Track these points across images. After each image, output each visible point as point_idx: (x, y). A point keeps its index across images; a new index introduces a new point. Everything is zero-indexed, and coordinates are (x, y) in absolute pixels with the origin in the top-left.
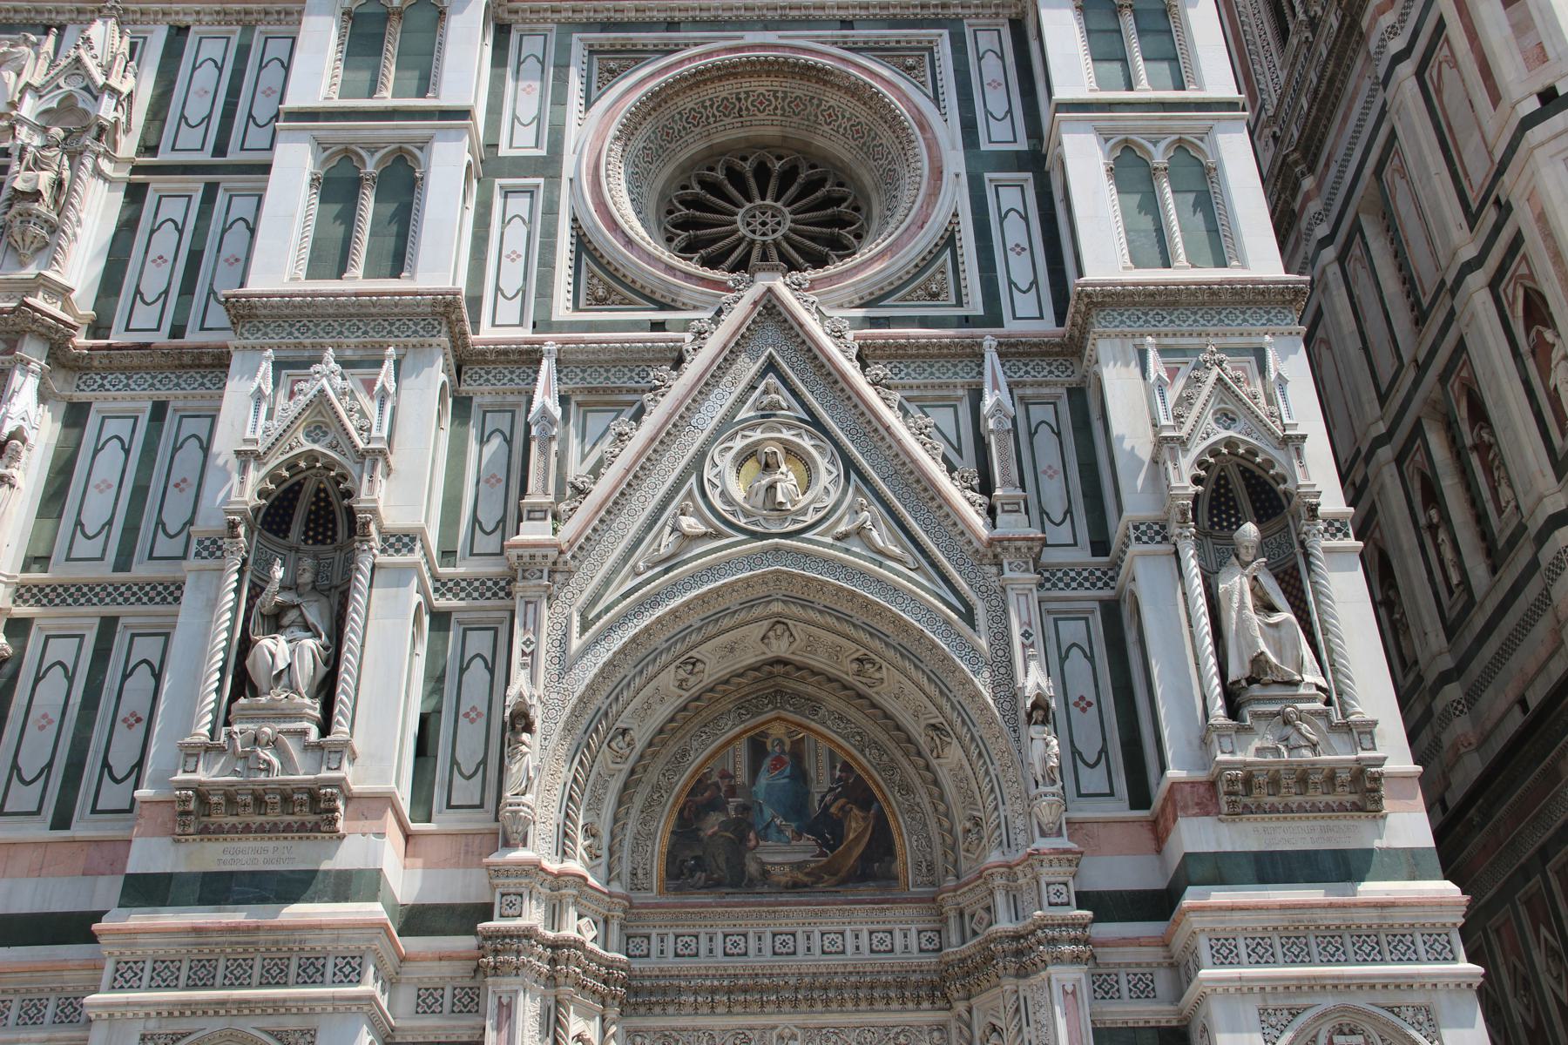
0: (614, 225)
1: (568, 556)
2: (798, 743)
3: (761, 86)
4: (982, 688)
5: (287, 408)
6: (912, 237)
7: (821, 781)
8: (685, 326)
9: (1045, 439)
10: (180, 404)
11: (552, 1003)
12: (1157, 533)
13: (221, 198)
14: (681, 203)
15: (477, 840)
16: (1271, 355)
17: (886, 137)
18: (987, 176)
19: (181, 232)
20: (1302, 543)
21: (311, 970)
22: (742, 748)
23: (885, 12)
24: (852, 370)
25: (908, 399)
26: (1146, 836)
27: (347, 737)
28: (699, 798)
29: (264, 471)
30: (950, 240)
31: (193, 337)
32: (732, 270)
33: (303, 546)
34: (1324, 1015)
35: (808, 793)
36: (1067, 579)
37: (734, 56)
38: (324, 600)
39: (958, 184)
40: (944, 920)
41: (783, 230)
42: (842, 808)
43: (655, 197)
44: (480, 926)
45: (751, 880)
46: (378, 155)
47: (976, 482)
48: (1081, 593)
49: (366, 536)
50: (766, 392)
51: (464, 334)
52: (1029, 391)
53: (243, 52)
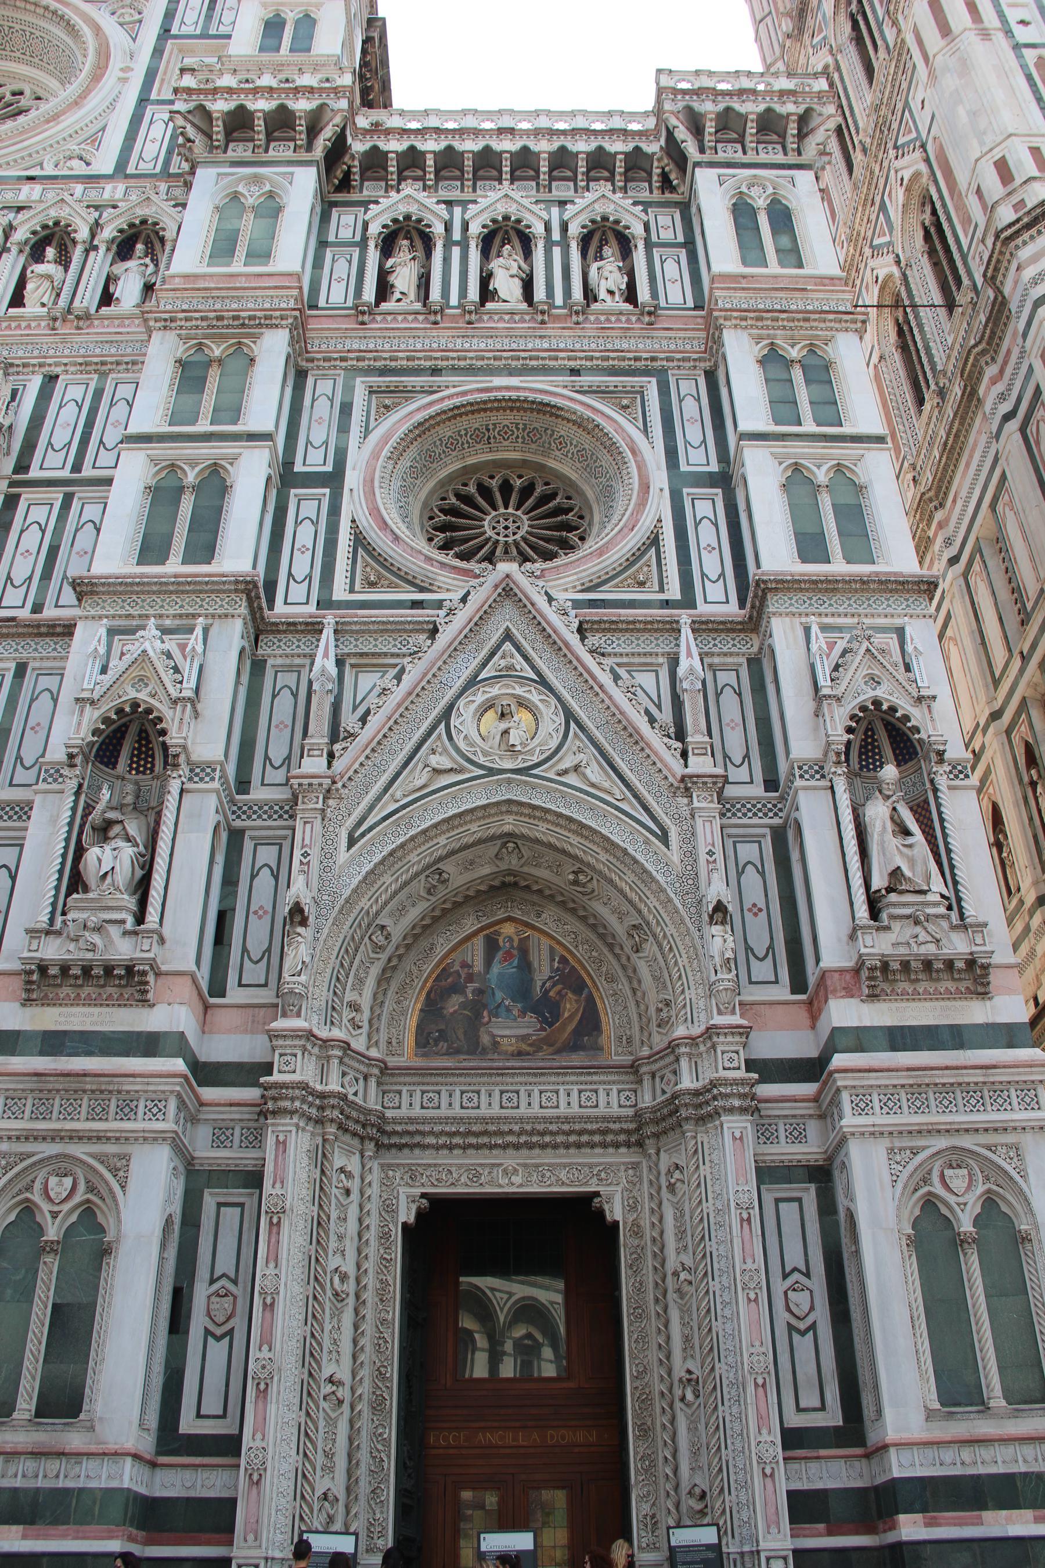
0: (384, 525)
1: (340, 785)
2: (524, 941)
3: (506, 419)
4: (673, 896)
5: (117, 665)
6: (624, 538)
7: (543, 970)
8: (439, 604)
9: (729, 699)
10: (37, 664)
11: (320, 1140)
12: (817, 772)
13: (76, 505)
14: (441, 511)
15: (263, 1011)
16: (908, 631)
17: (605, 459)
18: (685, 491)
19: (44, 532)
20: (932, 781)
21: (127, 1110)
22: (479, 942)
23: (606, 363)
24: (574, 639)
25: (618, 665)
26: (803, 1015)
27: (157, 926)
28: (443, 983)
29: (97, 714)
30: (654, 541)
31: (49, 612)
32: (479, 562)
33: (128, 776)
35: (532, 979)
37: (484, 396)
38: (143, 818)
39: (661, 497)
40: (640, 1082)
42: (559, 993)
43: (418, 505)
44: (262, 1080)
45: (484, 1049)
46: (197, 469)
47: (672, 730)
48: (755, 821)
49: (176, 766)
50: (503, 657)
51: (261, 608)
52: (716, 660)
53: (98, 394)
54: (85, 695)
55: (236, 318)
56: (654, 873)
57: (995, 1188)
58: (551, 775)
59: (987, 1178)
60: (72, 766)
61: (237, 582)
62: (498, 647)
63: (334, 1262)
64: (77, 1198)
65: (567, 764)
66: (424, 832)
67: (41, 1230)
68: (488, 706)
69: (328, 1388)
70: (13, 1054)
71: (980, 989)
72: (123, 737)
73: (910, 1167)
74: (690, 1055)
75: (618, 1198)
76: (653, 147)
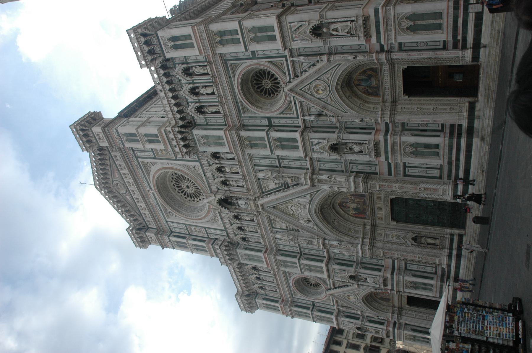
0: (278, 109)
2: (357, 80)
5: (322, 151)
22: (358, 87)
29: (331, 153)
34: (399, 27)
38: (347, 144)
41: (268, 81)
43: (267, 100)
52: (298, 52)
54: (329, 155)
58: (329, 82)
59: (403, 19)
64: (409, 147)
66: (343, 101)
67: (414, 151)
68: (316, 92)
70: (388, 157)
73: (401, 32)
74: (380, 60)
76: (160, 65)
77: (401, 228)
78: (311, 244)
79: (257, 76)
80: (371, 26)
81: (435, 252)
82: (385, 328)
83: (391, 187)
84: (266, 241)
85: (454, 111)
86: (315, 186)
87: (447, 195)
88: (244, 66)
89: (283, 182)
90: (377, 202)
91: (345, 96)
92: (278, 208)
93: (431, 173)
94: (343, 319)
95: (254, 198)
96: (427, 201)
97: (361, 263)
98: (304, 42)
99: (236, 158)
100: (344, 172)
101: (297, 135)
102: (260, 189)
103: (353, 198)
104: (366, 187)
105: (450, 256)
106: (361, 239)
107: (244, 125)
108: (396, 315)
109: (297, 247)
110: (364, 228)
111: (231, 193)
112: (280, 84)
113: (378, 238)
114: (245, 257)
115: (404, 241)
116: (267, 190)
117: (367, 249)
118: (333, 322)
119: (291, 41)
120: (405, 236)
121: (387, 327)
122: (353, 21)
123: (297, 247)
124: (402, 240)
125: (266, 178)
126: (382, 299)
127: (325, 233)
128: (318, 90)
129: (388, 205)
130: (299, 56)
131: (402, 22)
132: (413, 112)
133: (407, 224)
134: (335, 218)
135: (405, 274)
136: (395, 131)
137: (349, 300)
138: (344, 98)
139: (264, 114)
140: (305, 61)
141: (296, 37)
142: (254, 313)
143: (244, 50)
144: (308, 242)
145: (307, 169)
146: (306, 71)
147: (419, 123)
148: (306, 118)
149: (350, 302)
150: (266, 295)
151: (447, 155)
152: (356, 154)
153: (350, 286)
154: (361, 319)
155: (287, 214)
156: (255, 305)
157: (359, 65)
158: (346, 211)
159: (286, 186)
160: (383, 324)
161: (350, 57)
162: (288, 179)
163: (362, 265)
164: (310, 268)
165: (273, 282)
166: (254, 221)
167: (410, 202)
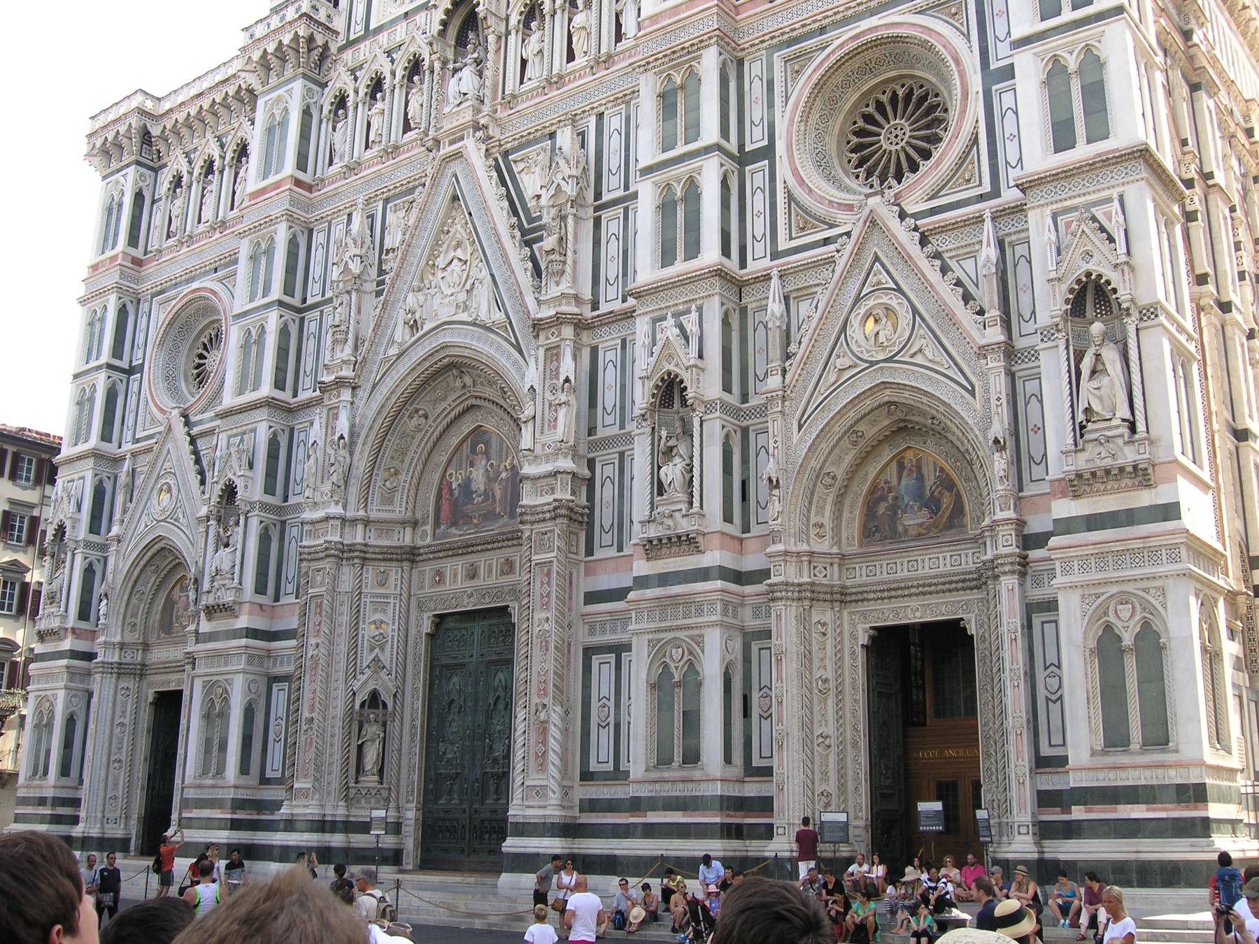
0: (802, 182)
1: (789, 392)
3: (876, 53)
4: (977, 432)
5: (656, 349)
7: (930, 479)
22: (894, 464)
24: (914, 249)
35: (924, 486)
36: (1029, 356)
38: (689, 439)
50: (875, 275)
52: (1014, 238)
54: (644, 374)
55: (683, 49)
56: (967, 418)
57: (1147, 615)
60: (645, 420)
61: (710, 272)
62: (872, 267)
63: (817, 674)
64: (685, 659)
65: (912, 351)
68: (868, 315)
69: (821, 740)
71: (1145, 483)
72: (673, 388)
74: (992, 537)
75: (973, 620)
77: (410, 650)
78: (335, 342)
79: (924, 98)
80: (1113, 496)
81: (334, 775)
82: (70, 625)
83: (545, 606)
84: (337, 181)
85: (817, 807)
86: (537, 337)
87: (526, 803)
88: (958, 42)
89: (544, 221)
90: (495, 558)
91: (858, 421)
92: (454, 213)
93: (602, 743)
94: (89, 475)
95: (482, 122)
96: (507, 733)
97: (283, 523)
98: (1051, 256)
99: (622, 46)
100: (589, 435)
101: (710, 254)
102: (516, 142)
103: (504, 475)
104: (540, 516)
105: (322, 826)
106: (362, 513)
107: (740, 62)
108: (116, 659)
109: (323, 295)
110: (403, 523)
111: (499, 38)
112: (894, 183)
113: (370, 574)
114: (277, 112)
115: (365, 665)
116: (516, 169)
117: (329, 538)
118: (76, 445)
119: (1054, 206)
120: (384, 667)
121: (73, 629)
122: (1133, 428)
123: (323, 295)
124: (367, 659)
125: (557, 159)
126: (170, 604)
127: (374, 386)
128: (876, 321)
129: (487, 600)
130: (1001, 244)
131: (1133, 607)
132: (811, 664)
133: (425, 671)
134: (431, 418)
135: (252, 677)
136: (742, 605)
137: (155, 493)
138: (852, 415)
139: (784, 134)
140: (980, 264)
141: (1068, 225)
142: (87, 162)
143: (1017, 34)
144: (343, 328)
145: (595, 306)
146: (945, 270)
147: (771, 689)
148: (775, 282)
149: (149, 499)
150: (153, 202)
151: (663, 794)
152: (652, 473)
153: (203, 493)
154: (94, 538)
155: (437, 244)
156: (115, 165)
157: (970, 463)
158: (458, 455)
159: (529, 237)
160: (84, 614)
161: (999, 428)
162: (556, 236)
163: (275, 525)
164: (252, 344)
165: (199, 222)
166: (404, 132)
167: (500, 675)
